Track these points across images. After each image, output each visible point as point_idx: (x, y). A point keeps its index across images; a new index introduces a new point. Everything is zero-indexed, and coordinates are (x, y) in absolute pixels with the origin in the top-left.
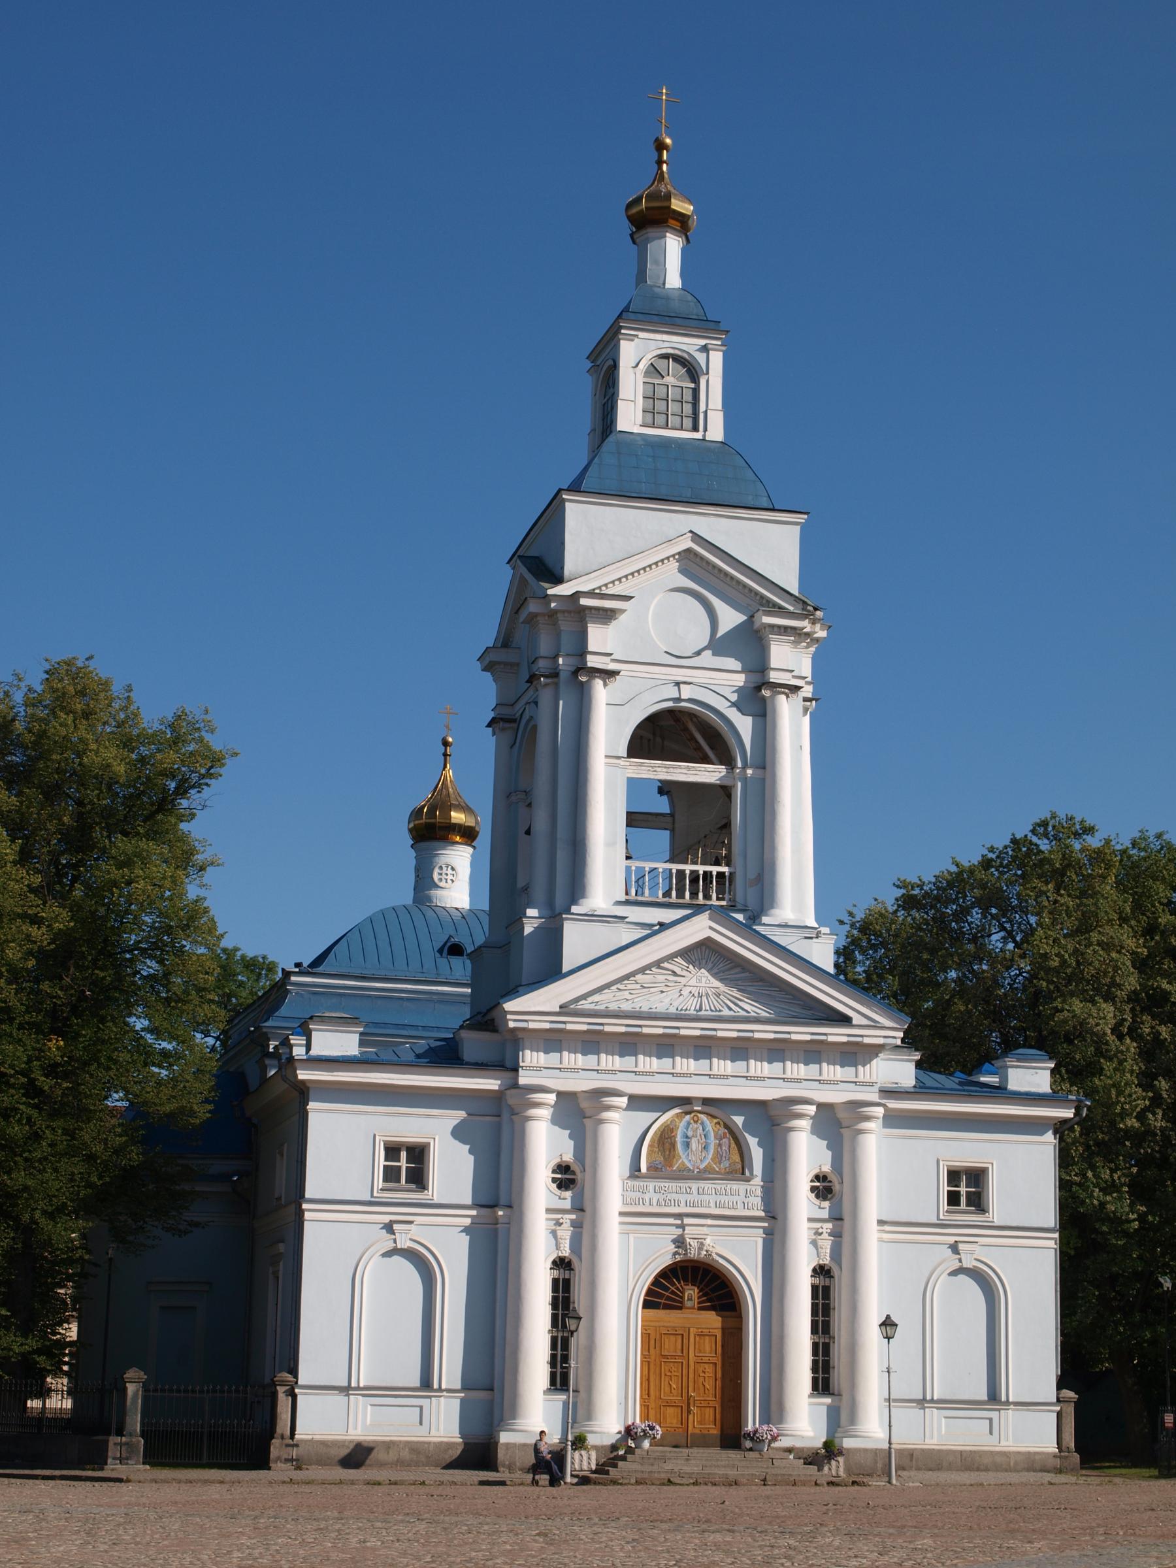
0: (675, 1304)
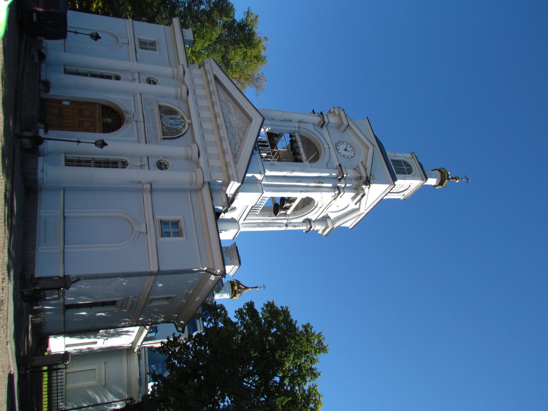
0: (104, 115)
